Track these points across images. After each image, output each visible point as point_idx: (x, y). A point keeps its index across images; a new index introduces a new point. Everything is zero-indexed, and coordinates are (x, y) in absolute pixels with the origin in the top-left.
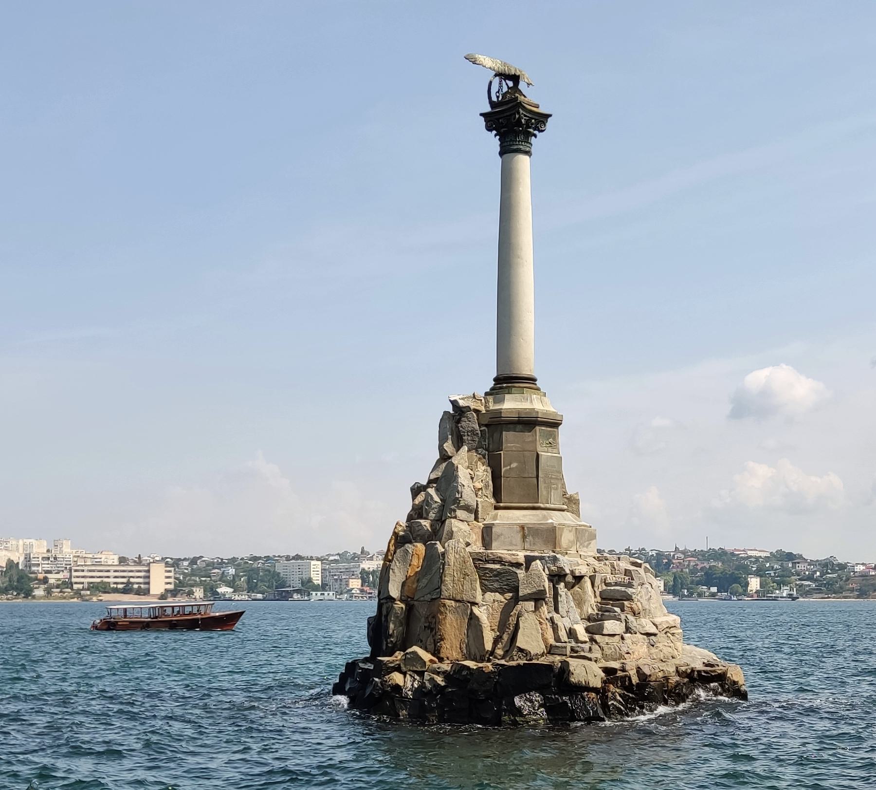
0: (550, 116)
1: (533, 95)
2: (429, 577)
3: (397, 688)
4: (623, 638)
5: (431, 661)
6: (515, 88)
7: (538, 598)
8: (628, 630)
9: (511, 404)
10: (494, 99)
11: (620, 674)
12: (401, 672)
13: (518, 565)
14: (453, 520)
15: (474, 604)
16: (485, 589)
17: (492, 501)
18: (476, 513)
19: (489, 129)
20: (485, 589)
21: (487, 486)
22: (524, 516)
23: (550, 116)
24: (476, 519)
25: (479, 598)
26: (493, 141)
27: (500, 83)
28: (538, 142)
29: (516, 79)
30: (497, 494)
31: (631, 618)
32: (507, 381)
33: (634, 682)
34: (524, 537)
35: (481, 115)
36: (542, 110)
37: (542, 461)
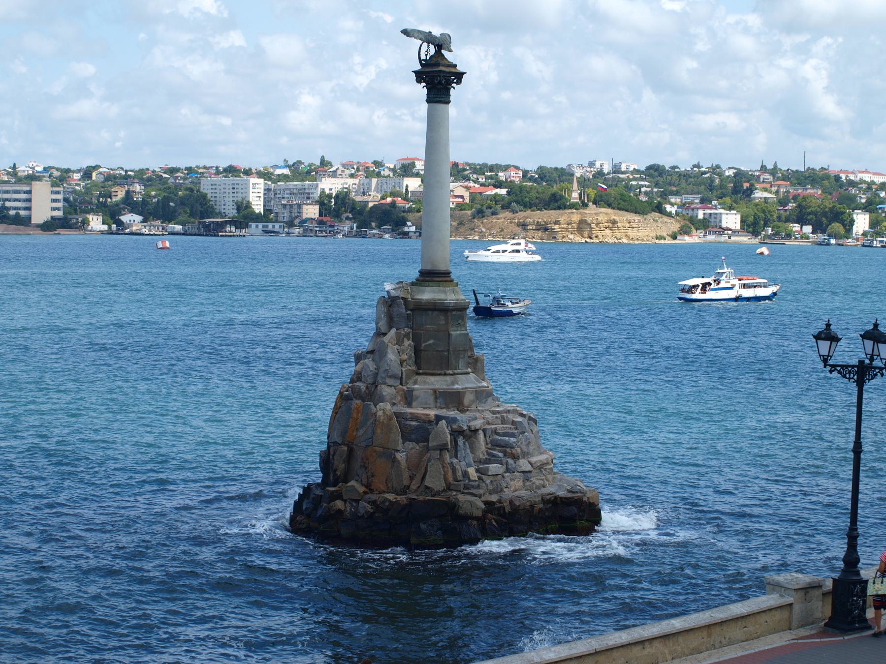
1: (454, 56)
2: (364, 429)
3: (340, 512)
4: (503, 477)
6: (438, 53)
7: (442, 448)
8: (508, 470)
9: (428, 294)
10: (423, 57)
11: (498, 505)
12: (343, 500)
13: (430, 422)
14: (383, 386)
15: (398, 451)
16: (405, 439)
17: (414, 368)
18: (401, 379)
19: (419, 81)
20: (405, 439)
21: (410, 358)
22: (437, 381)
24: (401, 384)
25: (400, 447)
26: (421, 90)
27: (429, 47)
28: (456, 92)
29: (441, 44)
30: (417, 363)
31: (510, 461)
33: (507, 510)
34: (436, 398)
36: (460, 68)
37: (453, 338)
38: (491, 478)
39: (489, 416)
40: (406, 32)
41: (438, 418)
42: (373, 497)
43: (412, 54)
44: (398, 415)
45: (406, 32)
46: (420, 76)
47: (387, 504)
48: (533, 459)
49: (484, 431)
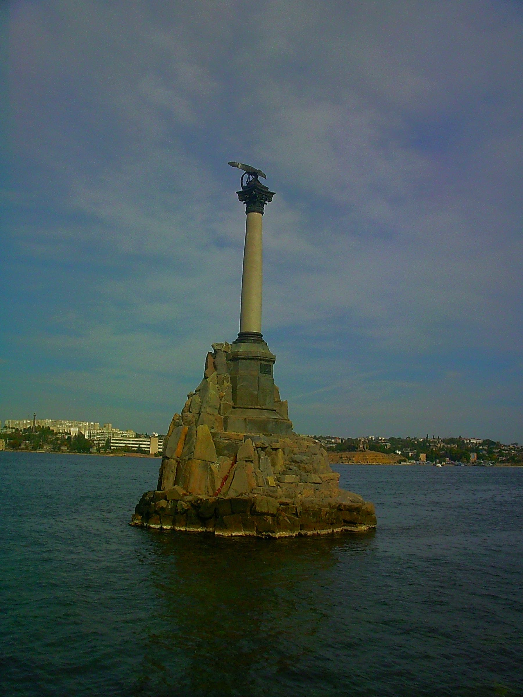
0: (275, 193)
3: (162, 508)
5: (185, 495)
12: (166, 499)
17: (232, 403)
18: (219, 410)
23: (275, 193)
24: (219, 413)
28: (267, 206)
31: (303, 473)
32: (244, 337)
35: (237, 193)
38: (287, 486)
39: (287, 440)
40: (232, 164)
41: (246, 437)
42: (189, 498)
43: (238, 180)
44: (214, 435)
45: (232, 164)
46: (242, 196)
47: (199, 502)
48: (322, 476)
49: (283, 450)
